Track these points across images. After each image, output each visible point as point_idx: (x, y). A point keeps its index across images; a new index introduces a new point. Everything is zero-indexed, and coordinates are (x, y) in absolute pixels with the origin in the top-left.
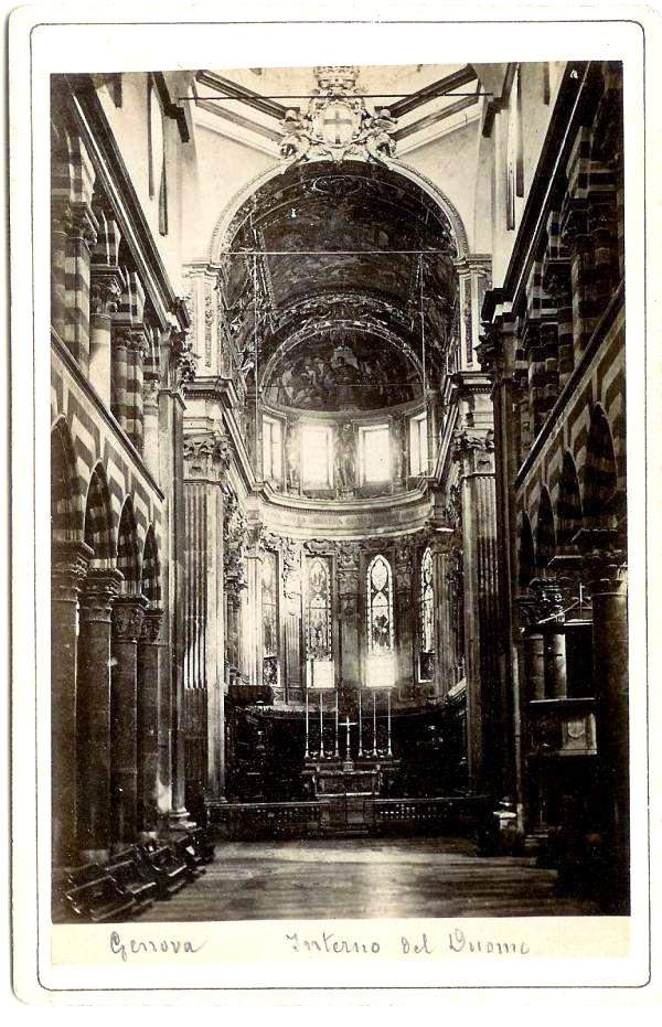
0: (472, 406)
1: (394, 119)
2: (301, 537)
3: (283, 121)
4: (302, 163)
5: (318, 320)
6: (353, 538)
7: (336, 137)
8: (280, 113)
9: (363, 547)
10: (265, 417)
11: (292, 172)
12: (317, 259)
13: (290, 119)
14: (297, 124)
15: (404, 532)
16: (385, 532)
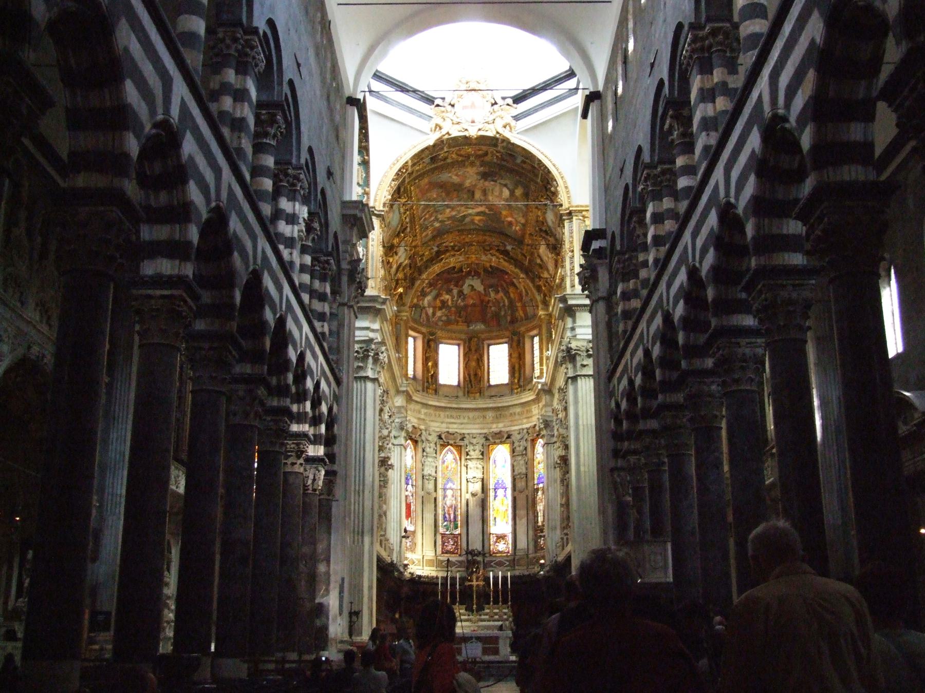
0: (574, 322)
1: (515, 105)
2: (438, 430)
3: (433, 106)
4: (447, 137)
5: (454, 255)
6: (479, 431)
7: (474, 119)
8: (429, 100)
9: (487, 439)
10: (411, 332)
11: (440, 143)
12: (453, 209)
13: (438, 105)
14: (442, 109)
15: (520, 427)
16: (505, 427)
